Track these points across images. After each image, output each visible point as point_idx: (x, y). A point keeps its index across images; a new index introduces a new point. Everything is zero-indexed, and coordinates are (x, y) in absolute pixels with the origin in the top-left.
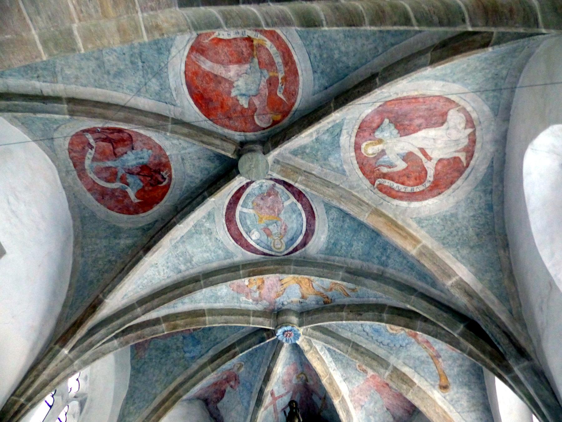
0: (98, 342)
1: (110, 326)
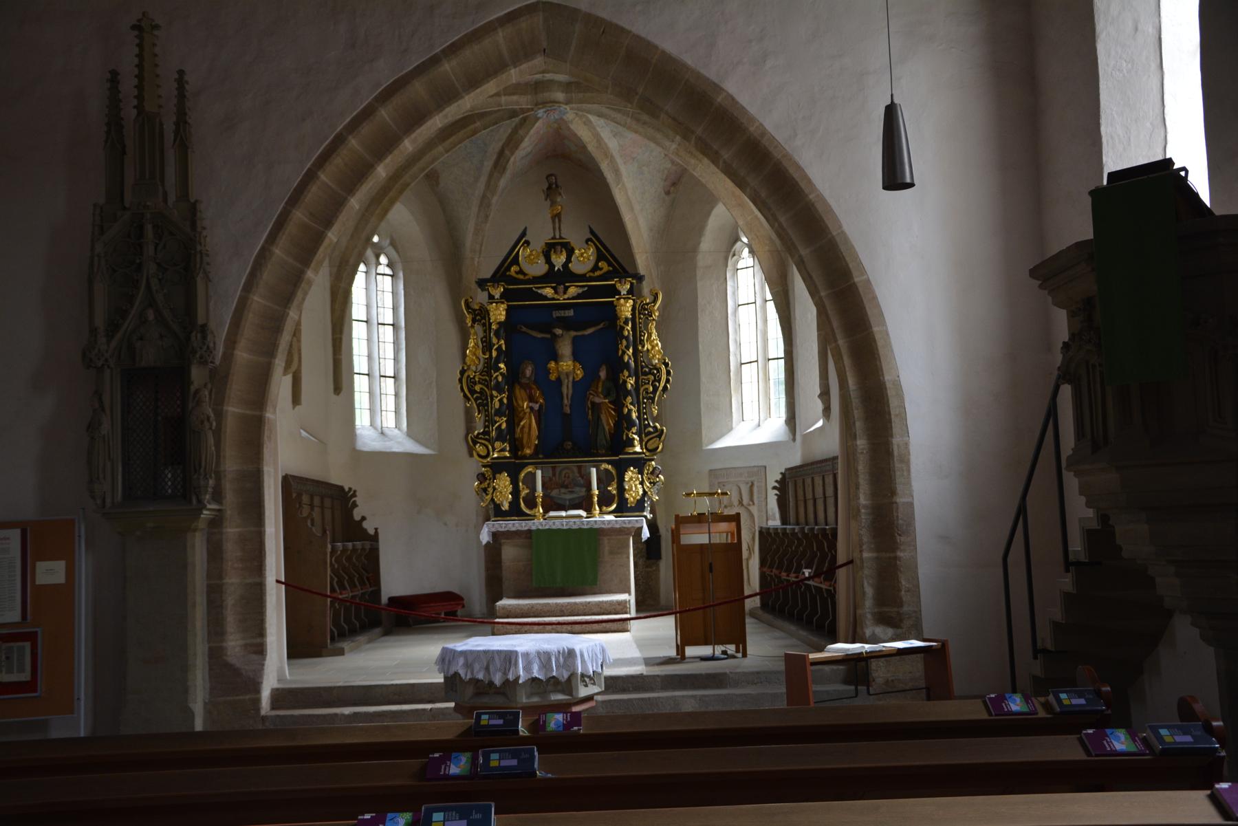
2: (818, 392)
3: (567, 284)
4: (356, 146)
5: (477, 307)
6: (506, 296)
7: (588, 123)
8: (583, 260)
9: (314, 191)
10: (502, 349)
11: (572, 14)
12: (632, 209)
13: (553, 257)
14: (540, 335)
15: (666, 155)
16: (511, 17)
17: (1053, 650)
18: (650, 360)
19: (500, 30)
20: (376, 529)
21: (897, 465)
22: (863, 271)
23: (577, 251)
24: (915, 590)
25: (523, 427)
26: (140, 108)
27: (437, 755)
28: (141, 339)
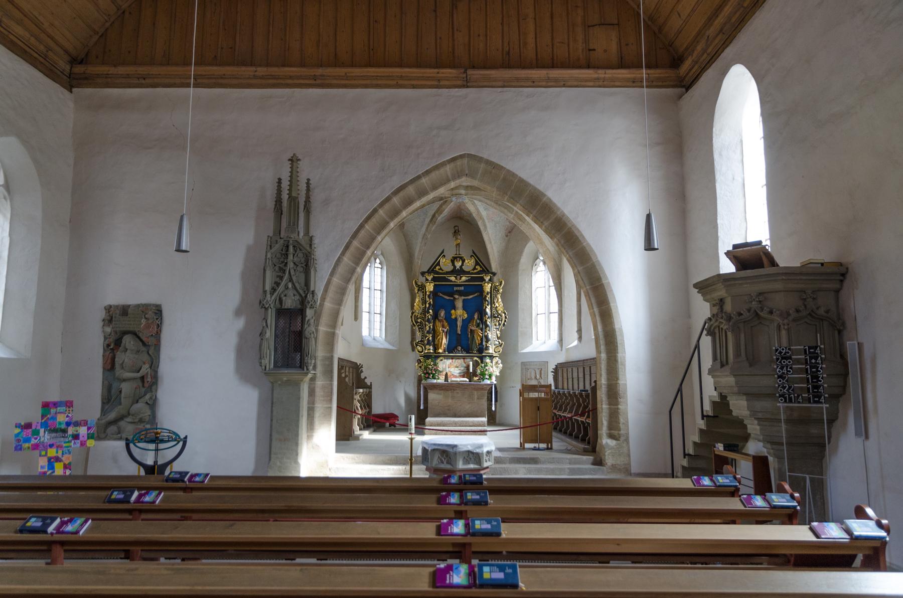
2: (576, 329)
3: (461, 275)
4: (383, 214)
5: (420, 284)
6: (434, 279)
7: (474, 204)
8: (469, 264)
9: (362, 233)
11: (480, 159)
12: (491, 243)
13: (456, 263)
14: (448, 298)
15: (507, 219)
16: (453, 160)
17: (693, 454)
18: (497, 311)
19: (448, 165)
20: (371, 383)
21: (620, 366)
22: (607, 279)
23: (466, 261)
24: (626, 424)
25: (439, 339)
26: (290, 194)
27: (444, 493)
28: (285, 296)
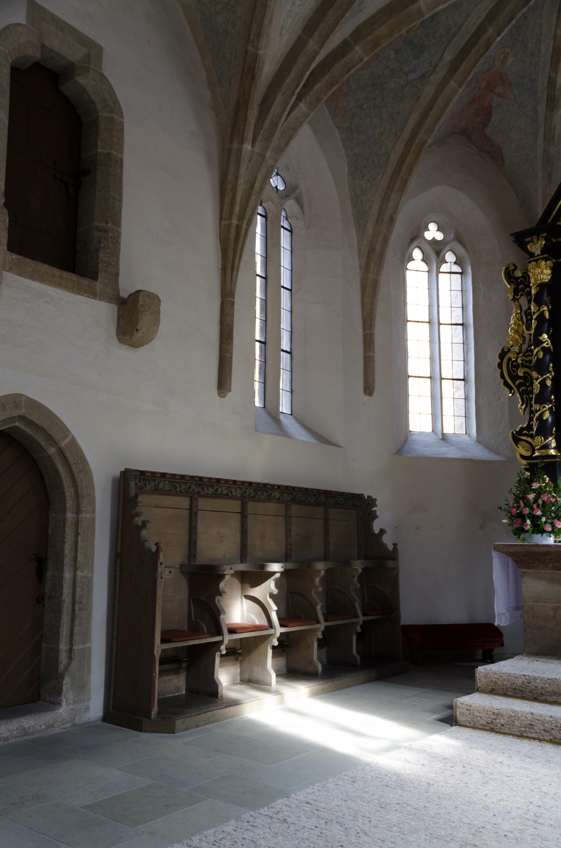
0: (281, 117)
1: (284, 88)
10: (545, 317)
20: (395, 545)
